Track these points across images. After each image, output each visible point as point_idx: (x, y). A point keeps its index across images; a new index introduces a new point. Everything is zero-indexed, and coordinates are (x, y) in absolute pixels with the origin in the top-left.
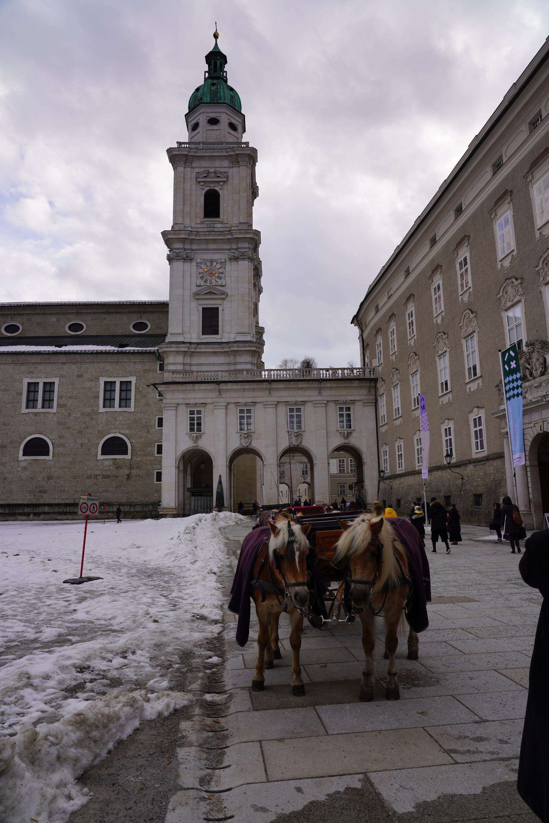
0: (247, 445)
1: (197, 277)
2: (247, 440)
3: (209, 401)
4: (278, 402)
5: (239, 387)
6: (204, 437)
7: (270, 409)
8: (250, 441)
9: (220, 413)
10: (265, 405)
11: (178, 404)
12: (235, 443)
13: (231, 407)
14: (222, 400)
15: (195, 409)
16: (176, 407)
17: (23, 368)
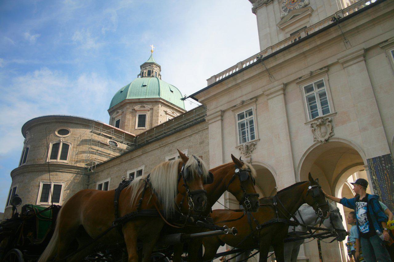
0: (327, 137)
1: (281, 12)
2: (323, 129)
3: (259, 92)
4: (367, 50)
5: (294, 54)
6: (259, 146)
7: (354, 66)
8: (329, 131)
9: (277, 103)
10: (344, 63)
11: (223, 112)
12: (306, 140)
13: (291, 89)
14: (276, 83)
15: (244, 111)
16: (222, 116)
17: (166, 149)
